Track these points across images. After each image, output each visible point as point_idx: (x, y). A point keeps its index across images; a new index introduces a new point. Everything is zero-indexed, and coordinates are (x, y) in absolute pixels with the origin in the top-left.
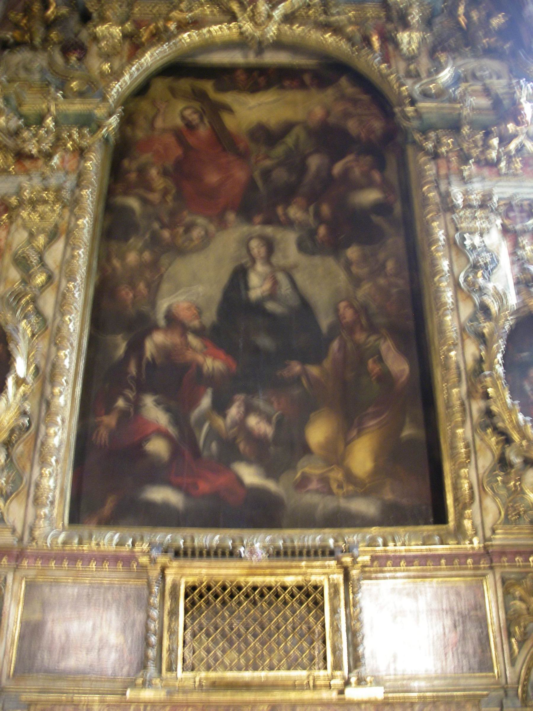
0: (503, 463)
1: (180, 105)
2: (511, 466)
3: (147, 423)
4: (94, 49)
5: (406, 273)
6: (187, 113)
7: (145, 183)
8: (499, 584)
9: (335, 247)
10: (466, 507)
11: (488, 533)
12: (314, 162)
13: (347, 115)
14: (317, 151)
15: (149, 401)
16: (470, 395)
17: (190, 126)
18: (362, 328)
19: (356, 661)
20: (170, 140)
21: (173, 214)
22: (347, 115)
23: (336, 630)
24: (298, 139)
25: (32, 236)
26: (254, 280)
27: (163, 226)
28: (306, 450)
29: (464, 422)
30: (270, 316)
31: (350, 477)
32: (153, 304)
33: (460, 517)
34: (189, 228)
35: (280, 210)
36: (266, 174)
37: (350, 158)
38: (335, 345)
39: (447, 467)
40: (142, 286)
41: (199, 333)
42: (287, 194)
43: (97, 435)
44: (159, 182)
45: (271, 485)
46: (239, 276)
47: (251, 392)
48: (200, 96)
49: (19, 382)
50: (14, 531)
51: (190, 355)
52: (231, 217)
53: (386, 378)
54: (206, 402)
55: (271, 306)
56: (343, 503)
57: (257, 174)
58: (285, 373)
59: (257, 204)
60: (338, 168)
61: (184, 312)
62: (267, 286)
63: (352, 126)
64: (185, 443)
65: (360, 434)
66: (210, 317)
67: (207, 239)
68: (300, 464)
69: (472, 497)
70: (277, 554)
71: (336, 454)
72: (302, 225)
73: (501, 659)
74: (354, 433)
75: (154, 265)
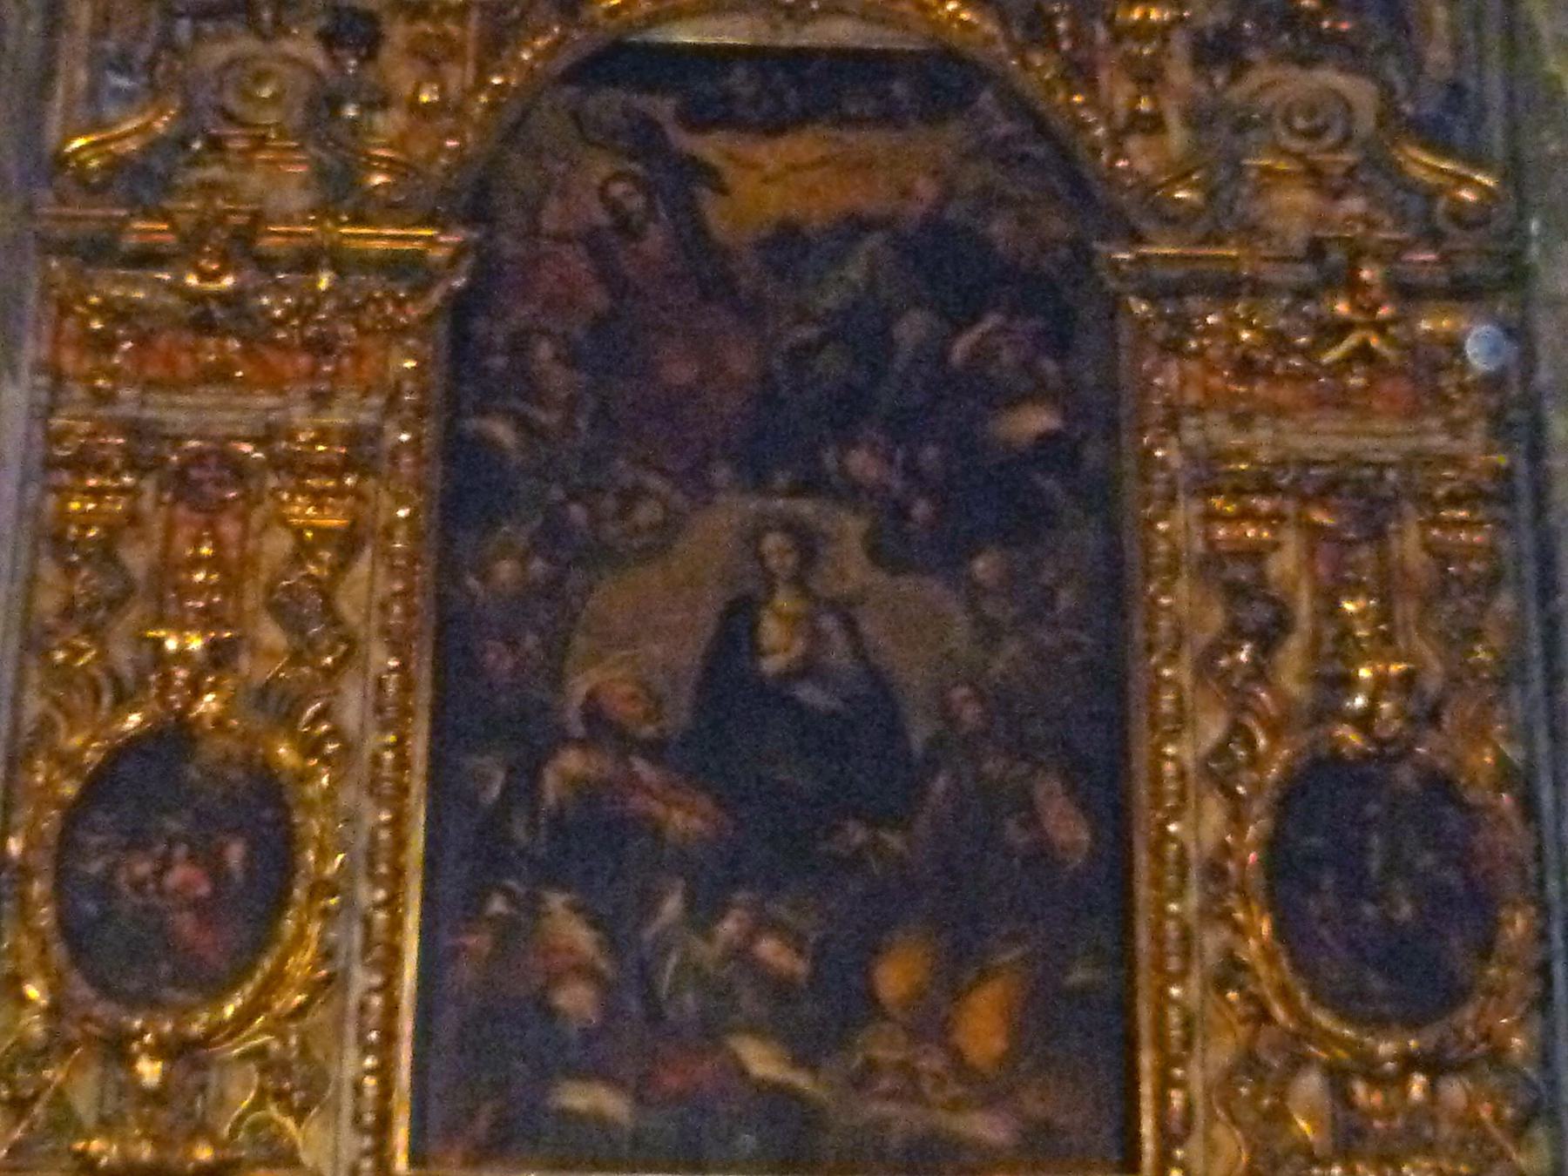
1: (602, 167)
6: (618, 189)
9: (950, 555)
10: (1180, 1141)
12: (912, 328)
13: (989, 199)
15: (556, 901)
16: (1204, 913)
17: (625, 226)
20: (577, 261)
22: (989, 199)
25: (303, 552)
26: (772, 631)
27: (573, 497)
34: (631, 497)
35: (829, 459)
36: (801, 355)
37: (992, 321)
38: (941, 783)
39: (1147, 1060)
40: (530, 641)
41: (655, 750)
42: (846, 413)
44: (559, 380)
45: (802, 1080)
46: (739, 618)
48: (645, 139)
51: (638, 802)
52: (721, 473)
53: (1042, 854)
54: (672, 906)
55: (808, 693)
56: (942, 1118)
59: (778, 440)
60: (961, 348)
61: (622, 703)
62: (799, 646)
63: (999, 228)
65: (984, 976)
66: (679, 715)
67: (670, 527)
69: (1188, 1125)
71: (931, 1023)
74: (970, 976)
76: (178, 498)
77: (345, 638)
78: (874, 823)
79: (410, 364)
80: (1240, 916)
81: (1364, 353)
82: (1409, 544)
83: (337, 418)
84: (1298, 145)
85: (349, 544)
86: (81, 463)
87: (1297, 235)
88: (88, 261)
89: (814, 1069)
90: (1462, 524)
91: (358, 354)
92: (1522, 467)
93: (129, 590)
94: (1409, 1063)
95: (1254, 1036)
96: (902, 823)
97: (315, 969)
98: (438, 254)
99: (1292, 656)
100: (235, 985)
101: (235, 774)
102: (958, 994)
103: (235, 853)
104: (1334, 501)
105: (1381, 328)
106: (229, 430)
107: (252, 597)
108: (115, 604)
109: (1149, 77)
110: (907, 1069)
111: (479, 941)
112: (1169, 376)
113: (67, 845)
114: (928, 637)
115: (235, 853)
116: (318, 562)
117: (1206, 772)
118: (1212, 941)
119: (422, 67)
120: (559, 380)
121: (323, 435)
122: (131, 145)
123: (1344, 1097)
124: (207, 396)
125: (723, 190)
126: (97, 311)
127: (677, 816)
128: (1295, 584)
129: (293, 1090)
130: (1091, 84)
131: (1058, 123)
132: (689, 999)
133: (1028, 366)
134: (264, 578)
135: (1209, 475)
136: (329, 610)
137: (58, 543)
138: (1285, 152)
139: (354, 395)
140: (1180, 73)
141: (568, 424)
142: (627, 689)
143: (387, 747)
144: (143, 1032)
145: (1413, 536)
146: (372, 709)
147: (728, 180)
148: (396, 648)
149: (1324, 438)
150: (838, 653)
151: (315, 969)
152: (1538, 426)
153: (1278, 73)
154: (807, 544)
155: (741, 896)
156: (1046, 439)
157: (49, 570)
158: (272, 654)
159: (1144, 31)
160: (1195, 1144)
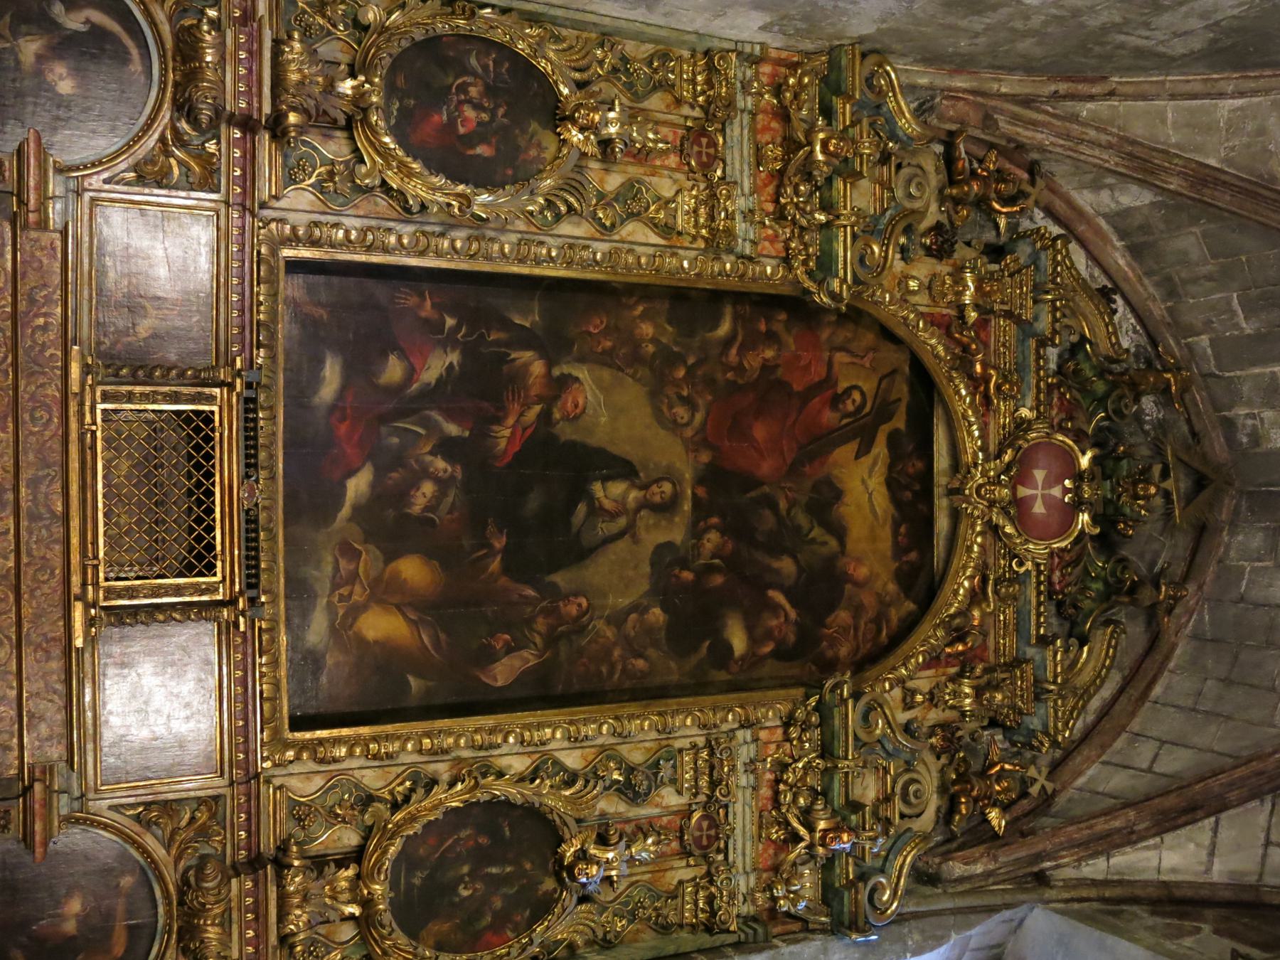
0: (368, 800)
1: (869, 386)
2: (363, 812)
4: (944, 268)
5: (627, 684)
6: (857, 396)
8: (210, 792)
9: (663, 591)
11: (277, 782)
12: (787, 566)
13: (858, 610)
14: (801, 570)
17: (836, 401)
18: (552, 629)
19: (121, 617)
20: (818, 372)
21: (710, 382)
22: (858, 610)
23: (156, 592)
24: (825, 543)
26: (617, 488)
27: (690, 371)
28: (391, 557)
29: (420, 752)
31: (355, 612)
32: (581, 360)
34: (689, 402)
36: (772, 504)
37: (793, 614)
38: (530, 592)
41: (545, 416)
42: (739, 529)
43: (405, 293)
44: (753, 362)
45: (345, 511)
46: (624, 469)
48: (884, 412)
49: (466, 201)
50: (276, 198)
52: (705, 457)
53: (488, 657)
54: (452, 429)
55: (582, 509)
57: (766, 489)
58: (491, 529)
59: (724, 490)
60: (779, 597)
62: (608, 504)
63: (842, 616)
66: (566, 432)
67: (674, 426)
68: (371, 547)
70: (251, 521)
71: (386, 593)
73: (119, 794)
75: (636, 358)
76: (689, 129)
77: (613, 225)
78: (505, 551)
79: (769, 270)
80: (459, 786)
81: (797, 839)
82: (682, 872)
83: (740, 226)
84: (898, 789)
85: (667, 230)
86: (711, 69)
87: (856, 793)
88: (825, 80)
89: (350, 520)
90: (696, 903)
91: (773, 239)
92: (731, 939)
93: (637, 97)
94: (367, 903)
95: (386, 801)
96: (506, 570)
97: (414, 197)
98: (835, 284)
99: (612, 805)
101: (533, 153)
103: (482, 150)
104: (705, 824)
105: (811, 847)
106: (729, 161)
108: (630, 86)
109: (933, 699)
111: (427, 310)
112: (771, 718)
114: (615, 584)
115: (482, 150)
116: (657, 211)
118: (442, 769)
119: (926, 281)
121: (730, 217)
122: (892, 105)
124: (747, 149)
125: (857, 457)
126: (800, 81)
127: (507, 433)
128: (657, 806)
129: (335, 183)
130: (926, 666)
131: (905, 648)
132: (395, 440)
133: (769, 635)
134: (647, 179)
136: (632, 216)
137: (665, 57)
138: (894, 782)
139: (752, 237)
140: (934, 716)
141: (728, 367)
142: (581, 402)
143: (549, 252)
144: (371, 83)
145: (686, 874)
147: (863, 459)
148: (609, 255)
149: (742, 815)
150: (605, 528)
151: (414, 197)
153: (935, 774)
154: (667, 508)
155: (459, 469)
156: (730, 648)
157: (649, 48)
158: (601, 181)
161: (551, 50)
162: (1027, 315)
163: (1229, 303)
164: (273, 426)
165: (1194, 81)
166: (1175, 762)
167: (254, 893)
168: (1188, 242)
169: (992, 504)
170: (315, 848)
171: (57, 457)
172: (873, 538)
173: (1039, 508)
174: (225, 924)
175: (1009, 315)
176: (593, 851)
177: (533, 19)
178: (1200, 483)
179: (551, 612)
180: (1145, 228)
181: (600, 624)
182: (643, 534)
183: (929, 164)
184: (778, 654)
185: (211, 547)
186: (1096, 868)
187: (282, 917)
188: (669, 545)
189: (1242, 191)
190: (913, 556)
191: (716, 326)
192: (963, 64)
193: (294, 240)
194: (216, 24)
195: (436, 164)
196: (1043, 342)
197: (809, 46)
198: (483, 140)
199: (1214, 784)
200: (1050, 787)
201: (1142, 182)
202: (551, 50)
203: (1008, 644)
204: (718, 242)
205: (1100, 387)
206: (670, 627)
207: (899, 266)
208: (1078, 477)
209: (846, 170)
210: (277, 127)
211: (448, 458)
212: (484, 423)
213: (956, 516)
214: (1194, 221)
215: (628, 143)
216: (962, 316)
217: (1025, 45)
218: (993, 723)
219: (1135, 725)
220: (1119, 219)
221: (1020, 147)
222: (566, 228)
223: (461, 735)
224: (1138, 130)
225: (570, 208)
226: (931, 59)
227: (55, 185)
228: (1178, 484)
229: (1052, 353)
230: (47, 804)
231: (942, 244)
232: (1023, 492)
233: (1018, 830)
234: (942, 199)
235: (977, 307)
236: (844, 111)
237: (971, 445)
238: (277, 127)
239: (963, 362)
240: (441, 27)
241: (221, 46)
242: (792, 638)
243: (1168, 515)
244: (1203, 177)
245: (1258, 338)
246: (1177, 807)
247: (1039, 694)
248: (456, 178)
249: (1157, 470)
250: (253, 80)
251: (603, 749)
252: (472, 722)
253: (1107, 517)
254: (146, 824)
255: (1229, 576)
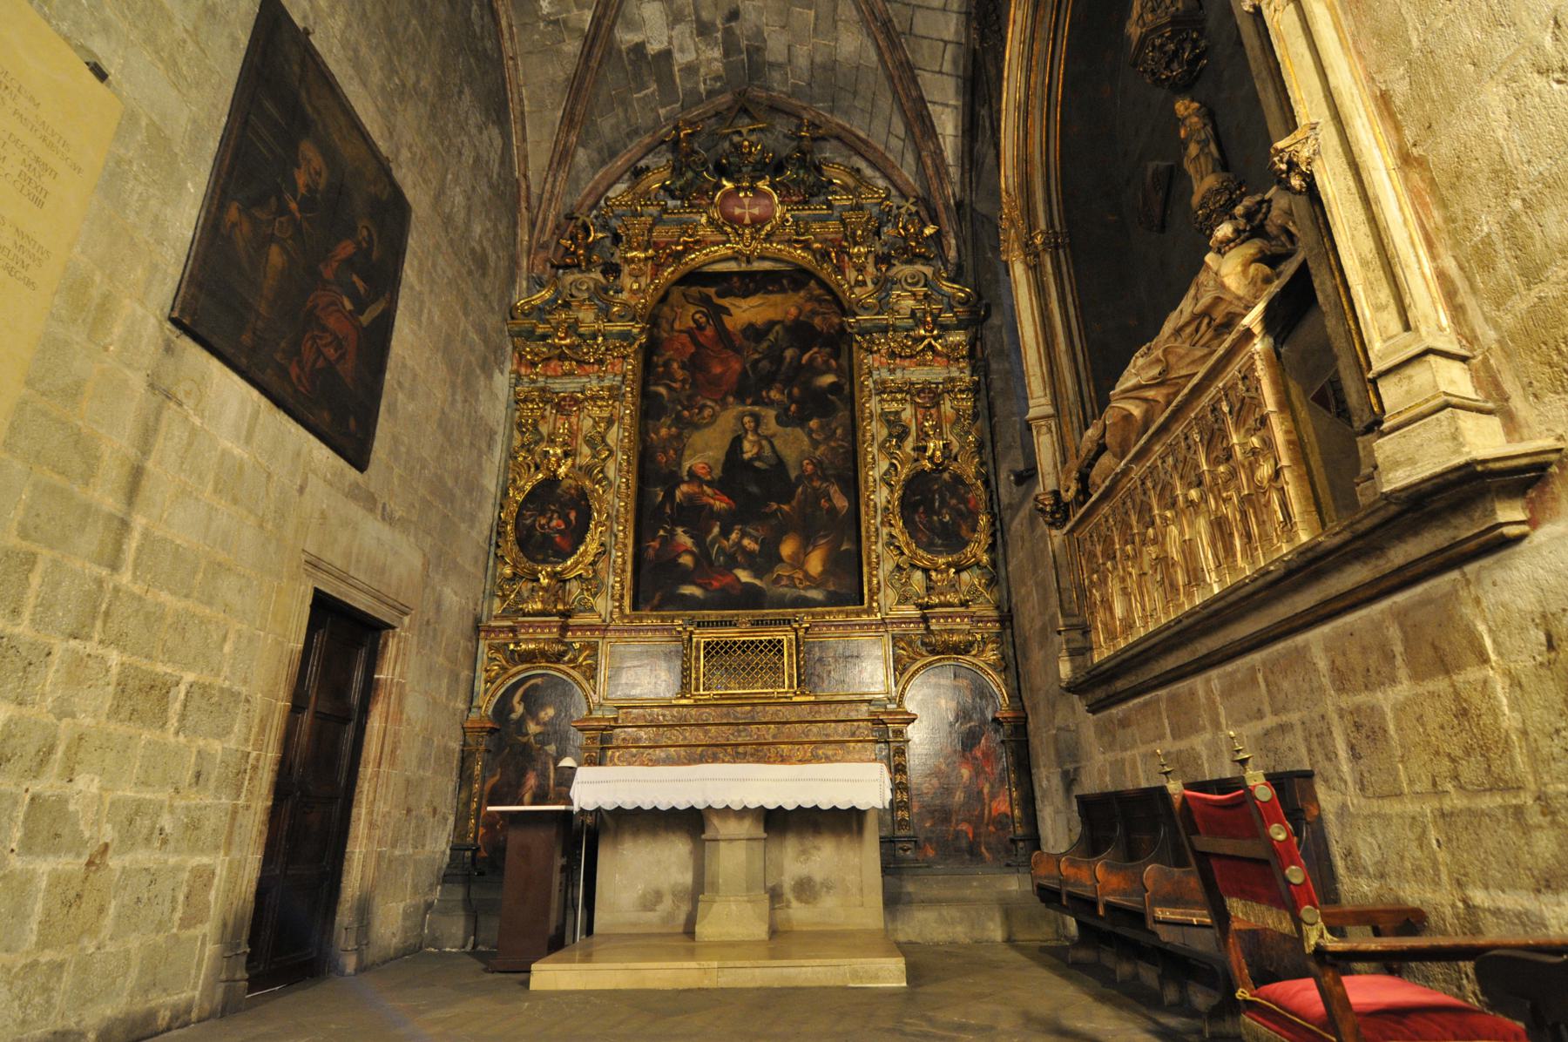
0: (899, 567)
1: (692, 309)
3: (679, 545)
4: (626, 269)
7: (669, 375)
9: (801, 421)
12: (789, 353)
15: (679, 530)
16: (882, 523)
17: (700, 328)
18: (820, 478)
20: (685, 338)
22: (814, 313)
25: (596, 423)
26: (746, 445)
27: (685, 408)
28: (781, 560)
30: (757, 470)
31: (807, 576)
32: (680, 465)
33: (871, 599)
34: (702, 408)
39: (865, 569)
41: (709, 484)
42: (768, 381)
44: (680, 374)
45: (757, 582)
46: (737, 442)
47: (744, 522)
48: (706, 301)
51: (705, 499)
52: (731, 399)
53: (833, 510)
54: (716, 530)
55: (757, 464)
59: (748, 389)
60: (806, 358)
61: (701, 471)
62: (755, 450)
63: (817, 321)
64: (703, 556)
65: (815, 547)
66: (717, 473)
67: (714, 416)
70: (756, 623)
71: (798, 562)
72: (779, 403)
75: (679, 437)
82: (947, 407)
83: (607, 383)
85: (610, 422)
86: (525, 401)
93: (542, 439)
94: (949, 565)
96: (788, 502)
98: (635, 331)
99: (909, 444)
100: (571, 555)
102: (806, 555)
103: (573, 516)
107: (580, 440)
108: (537, 443)
109: (861, 269)
110: (791, 578)
111: (655, 544)
112: (869, 360)
113: (519, 514)
114: (795, 446)
115: (573, 516)
117: (882, 479)
120: (680, 374)
123: (929, 578)
130: (843, 273)
133: (826, 362)
135: (882, 389)
137: (520, 425)
140: (871, 269)
141: (683, 388)
145: (948, 404)
146: (618, 472)
152: (987, 366)
154: (757, 419)
156: (833, 384)
157: (516, 433)
159: (859, 256)
160: (881, 594)
161: (520, 483)
162: (650, 220)
163: (638, 100)
164: (713, 615)
165: (515, 128)
166: (899, 127)
167: (938, 618)
168: (606, 125)
169: (753, 238)
170: (922, 592)
171: (725, 710)
172: (775, 305)
173: (756, 211)
174: (951, 632)
175: (650, 231)
176: (929, 453)
177: (505, 494)
178: (744, 111)
179: (810, 478)
180: (600, 151)
181: (818, 453)
182: (770, 432)
183: (569, 278)
184: (837, 358)
185: (770, 642)
186: (954, 172)
187: (951, 605)
188: (777, 417)
189: (575, 99)
190: (785, 282)
191: (661, 395)
192: (514, 262)
193: (620, 607)
194: (517, 644)
195: (581, 540)
196: (665, 210)
197: (510, 348)
198: (567, 515)
199: (907, 105)
200: (912, 200)
201: (573, 157)
202: (520, 483)
203: (833, 226)
204: (615, 394)
205: (690, 175)
206: (819, 417)
207: (624, 296)
208: (738, 189)
209: (573, 328)
210: (566, 614)
211: (730, 533)
212: (714, 515)
213: (762, 258)
214: (593, 123)
215: (565, 443)
216: (652, 258)
217: (502, 229)
218: (878, 233)
219: (881, 148)
220: (595, 166)
221: (558, 227)
222: (611, 473)
223: (871, 522)
224: (545, 161)
225: (602, 471)
226: (512, 280)
227: (598, 714)
228: (744, 125)
229: (671, 203)
230: (890, 713)
231: (612, 269)
232: (747, 221)
233: (934, 220)
234: (589, 270)
235: (646, 250)
236: (542, 329)
237: (723, 251)
238: (566, 614)
239: (678, 256)
240: (511, 537)
241: (527, 641)
242: (828, 350)
243: (761, 130)
244: (569, 121)
245: (658, 81)
246: (921, 125)
247: (859, 207)
248: (587, 529)
249: (736, 139)
250: (543, 626)
251: (879, 450)
252: (863, 518)
253: (760, 170)
254: (905, 669)
255: (795, 92)
